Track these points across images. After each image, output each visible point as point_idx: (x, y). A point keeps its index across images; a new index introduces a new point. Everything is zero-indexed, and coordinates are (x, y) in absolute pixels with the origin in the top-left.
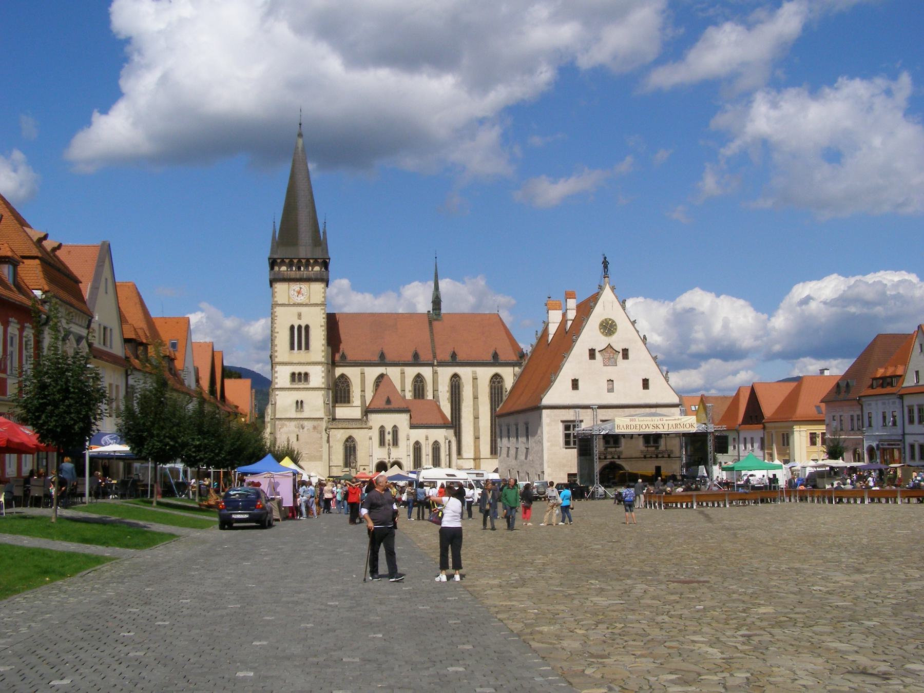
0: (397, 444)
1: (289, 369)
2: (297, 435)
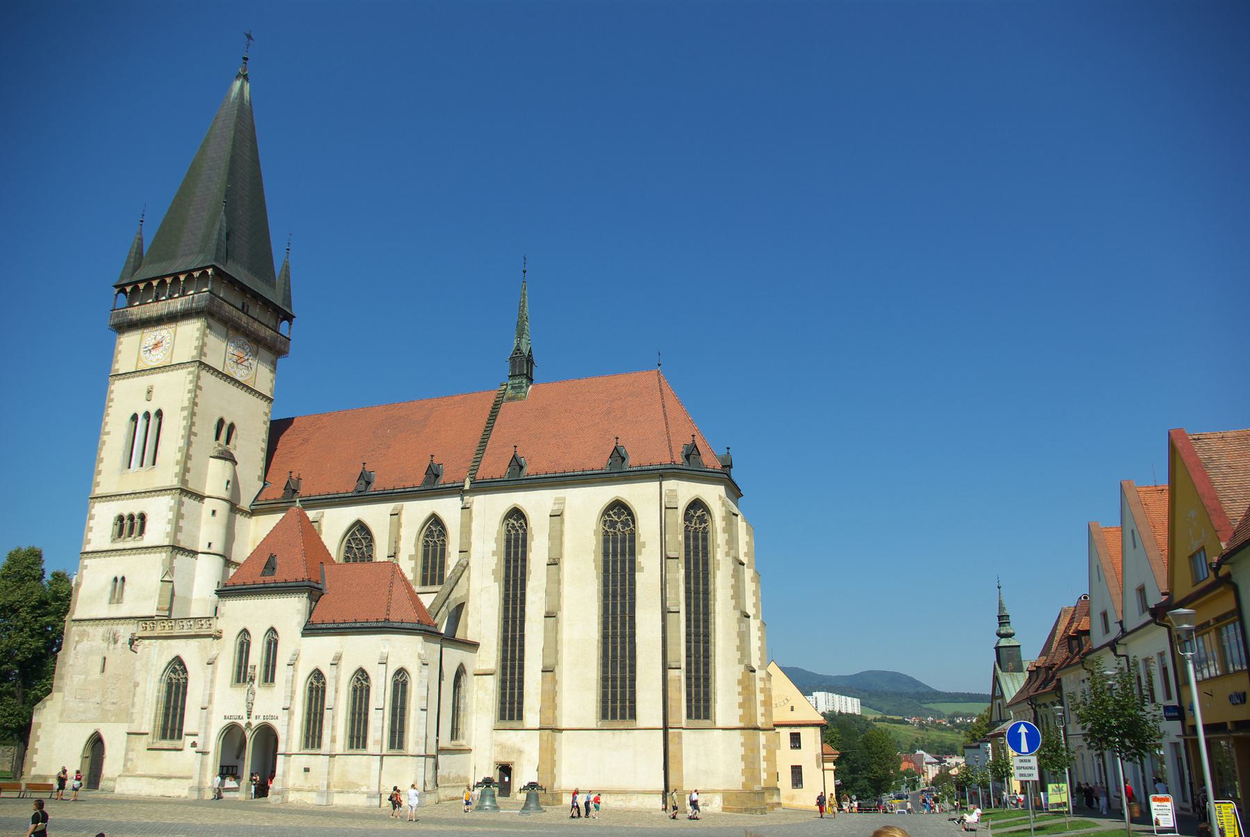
0: (273, 680)
2: (105, 659)
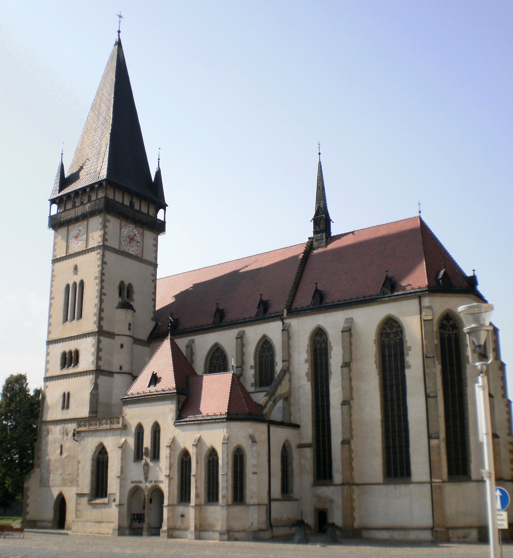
2: (62, 446)
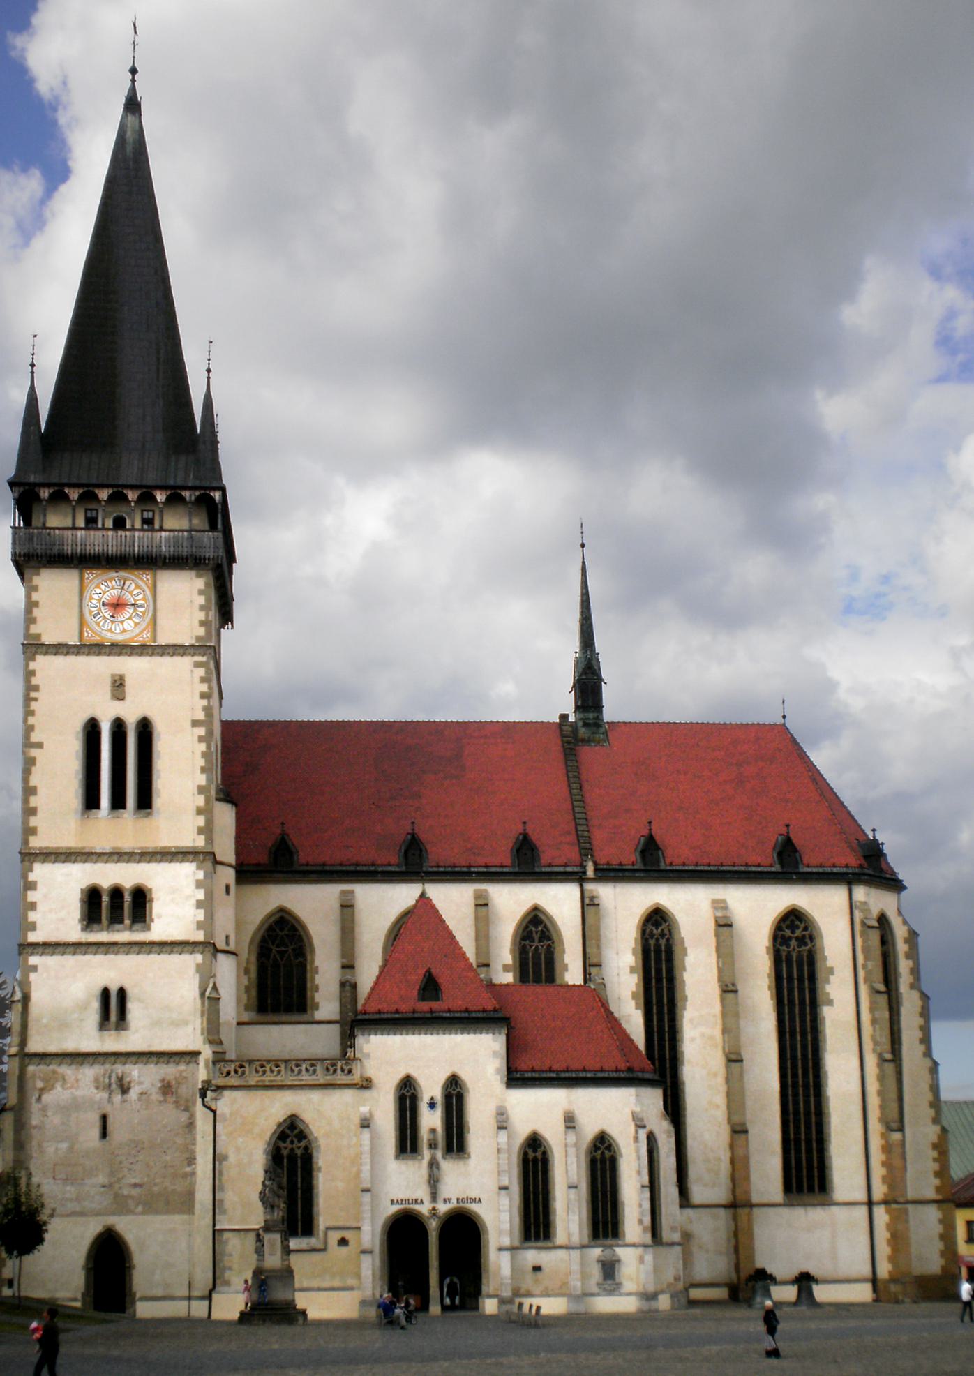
1: (77, 877)
